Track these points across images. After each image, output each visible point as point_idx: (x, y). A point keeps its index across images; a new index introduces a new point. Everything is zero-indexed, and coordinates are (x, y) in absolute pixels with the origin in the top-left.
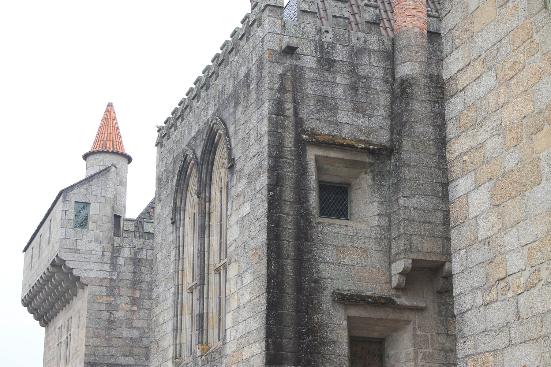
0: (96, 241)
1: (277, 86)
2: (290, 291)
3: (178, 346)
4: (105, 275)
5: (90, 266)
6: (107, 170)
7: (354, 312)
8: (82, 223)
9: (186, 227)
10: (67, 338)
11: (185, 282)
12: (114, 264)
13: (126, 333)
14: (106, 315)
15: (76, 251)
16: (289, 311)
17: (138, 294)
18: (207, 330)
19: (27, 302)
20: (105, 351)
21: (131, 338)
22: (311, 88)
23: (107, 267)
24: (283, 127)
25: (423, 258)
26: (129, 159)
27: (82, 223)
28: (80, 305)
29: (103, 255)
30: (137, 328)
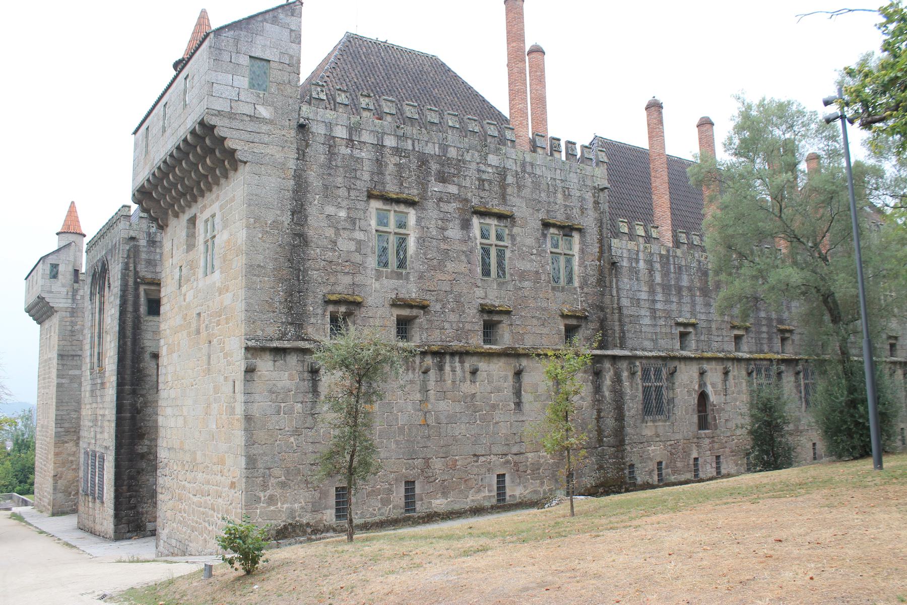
0: (63, 286)
2: (129, 354)
4: (69, 305)
6: (69, 244)
8: (54, 275)
14: (69, 328)
15: (51, 292)
16: (128, 362)
19: (28, 310)
20: (69, 348)
22: (143, 256)
23: (70, 301)
24: (128, 276)
26: (84, 236)
27: (54, 275)
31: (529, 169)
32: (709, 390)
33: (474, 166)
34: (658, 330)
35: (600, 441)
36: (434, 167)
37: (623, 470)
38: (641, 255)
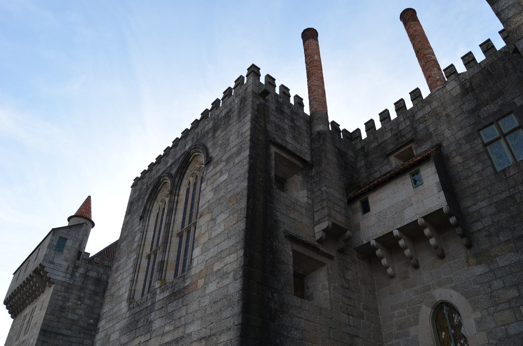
0: (66, 260)
1: (256, 109)
3: (133, 291)
4: (67, 280)
5: (59, 274)
7: (297, 248)
9: (150, 221)
10: (29, 319)
11: (145, 252)
12: (73, 275)
13: (70, 316)
14: (61, 303)
15: (52, 263)
17: (82, 295)
18: (166, 271)
21: (73, 320)
23: (68, 276)
25: (337, 223)
26: (93, 225)
28: (45, 298)
29: (68, 269)
30: (77, 314)
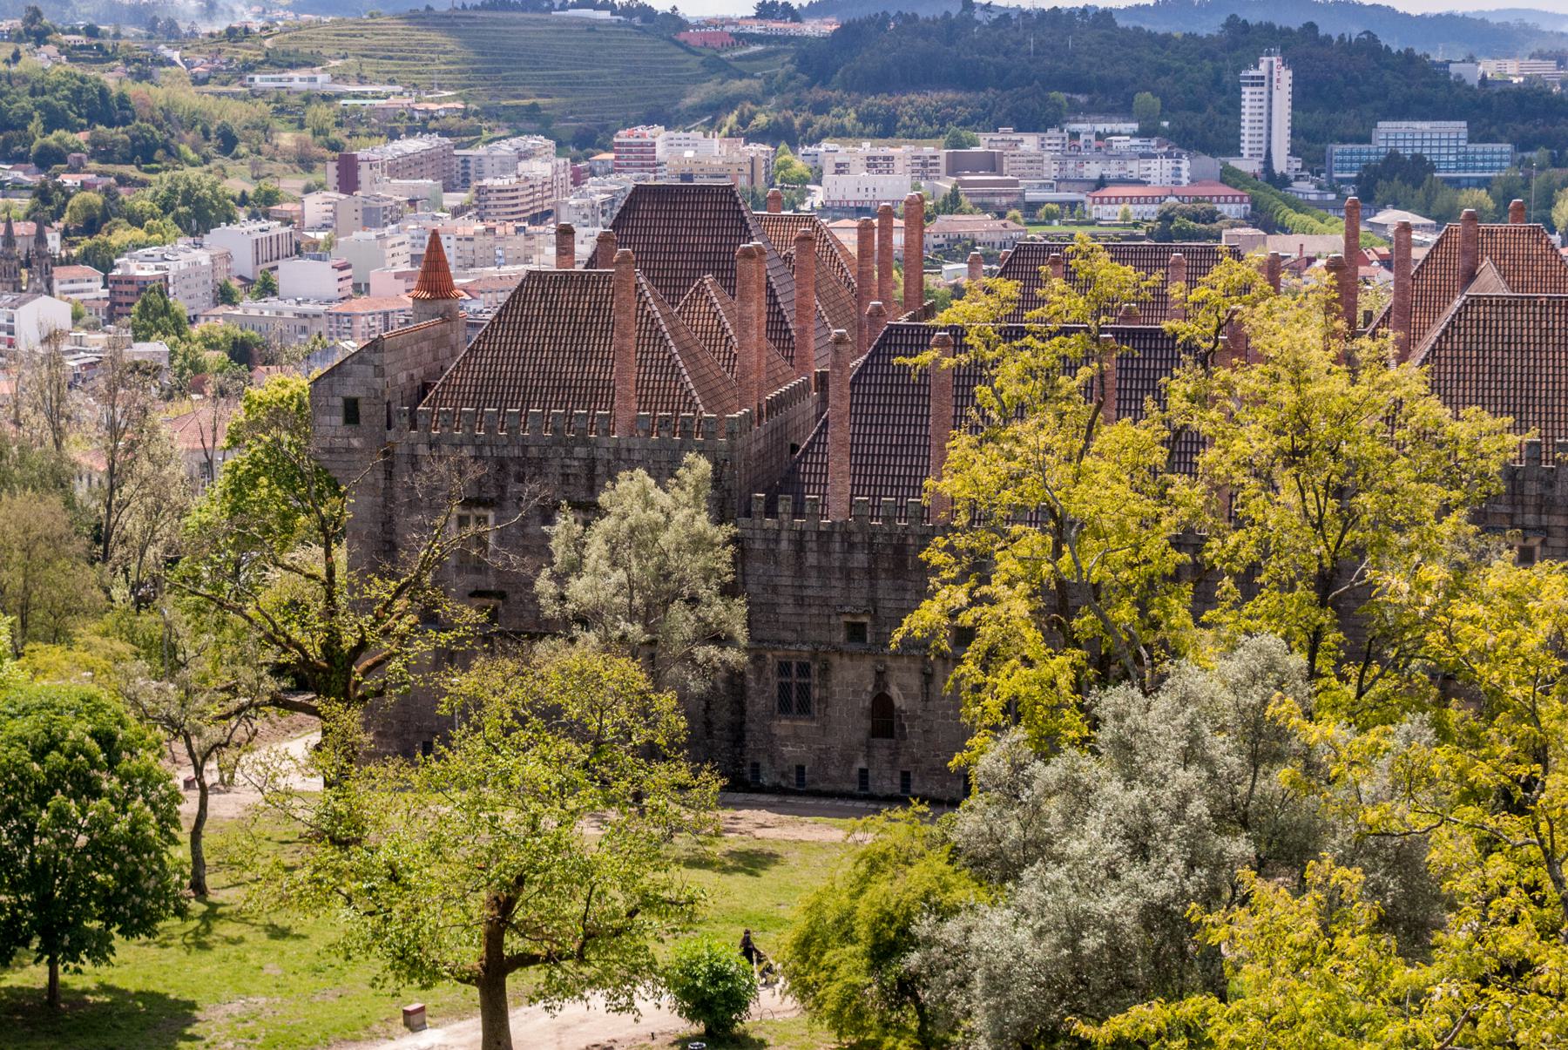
31: (624, 455)
32: (894, 691)
33: (557, 462)
34: (806, 619)
35: (709, 734)
36: (513, 468)
37: (741, 766)
38: (784, 535)
